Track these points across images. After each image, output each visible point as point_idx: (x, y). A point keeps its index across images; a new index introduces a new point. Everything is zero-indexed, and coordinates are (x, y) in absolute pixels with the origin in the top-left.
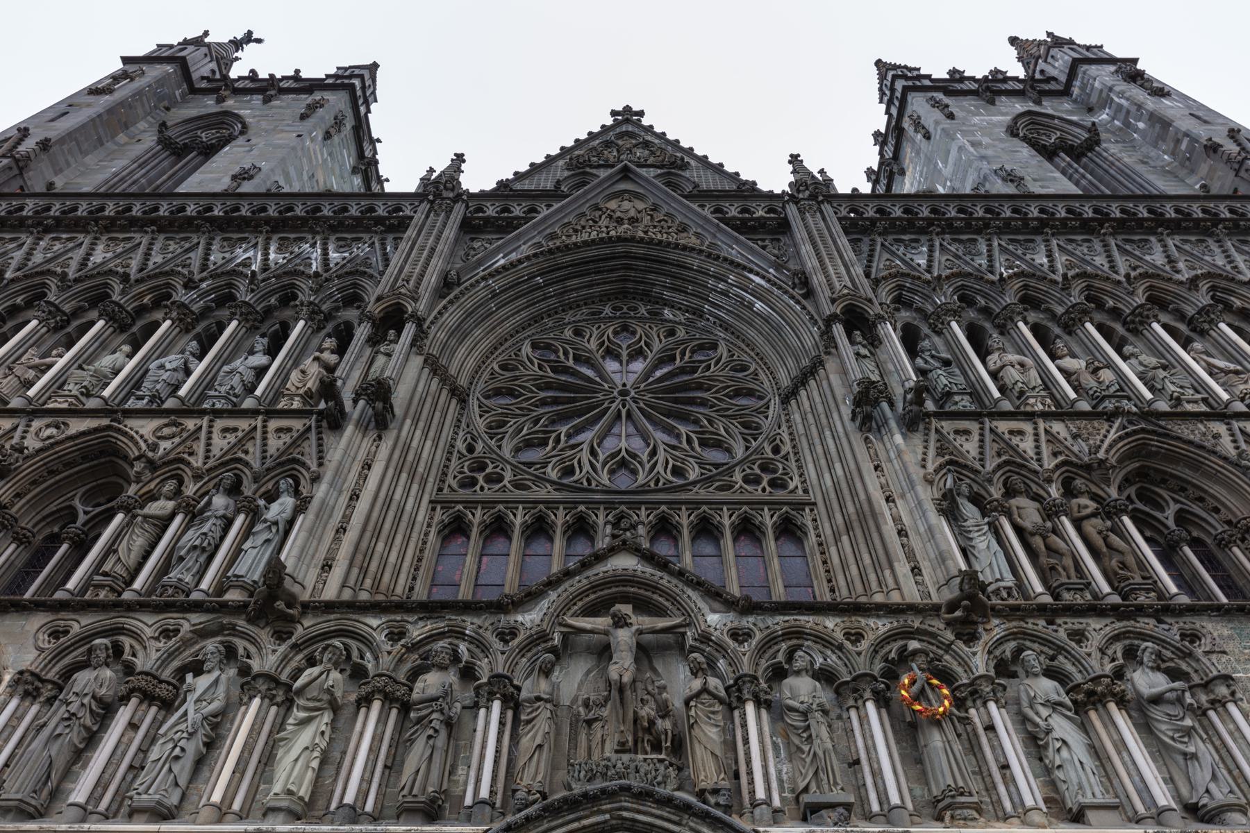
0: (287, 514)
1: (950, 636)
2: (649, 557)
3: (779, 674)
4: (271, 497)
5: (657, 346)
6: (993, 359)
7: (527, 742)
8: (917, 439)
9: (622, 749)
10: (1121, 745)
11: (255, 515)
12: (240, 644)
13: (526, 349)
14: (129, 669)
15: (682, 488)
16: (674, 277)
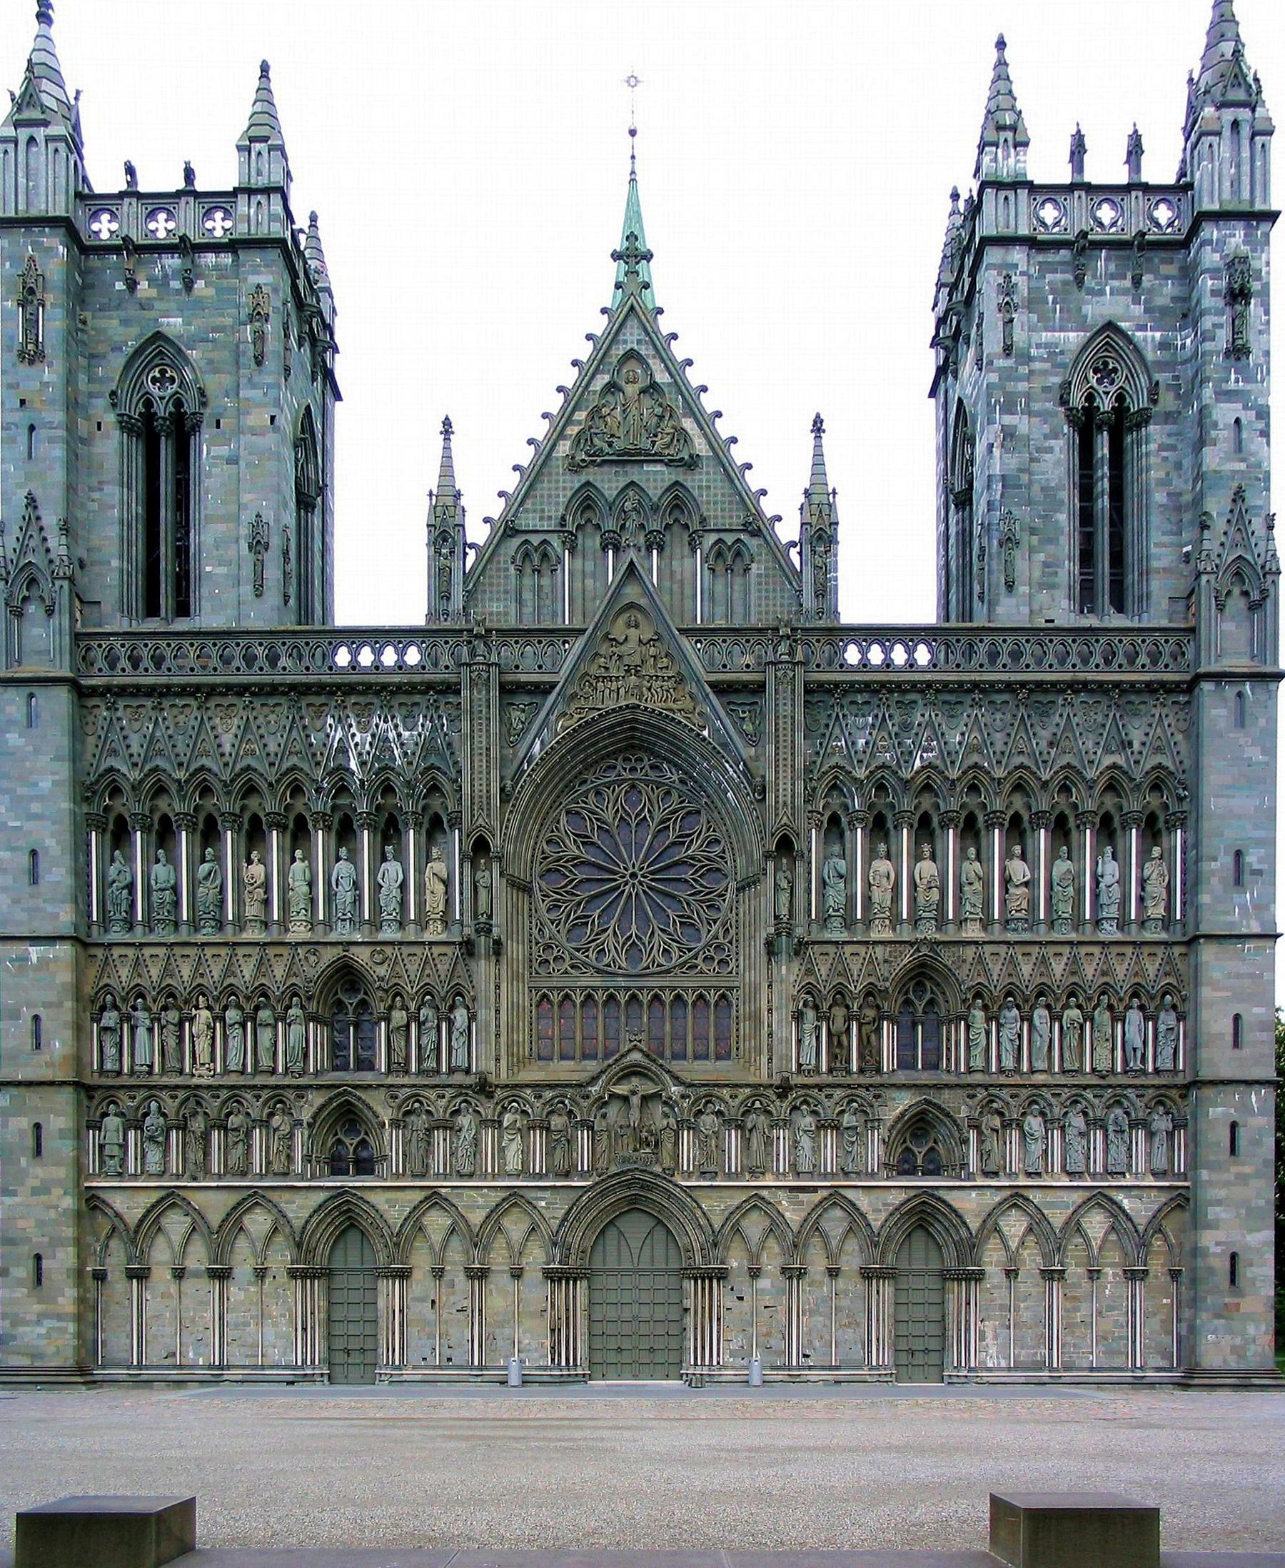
0: (466, 1024)
1: (774, 1098)
2: (647, 1056)
3: (700, 1112)
4: (452, 1008)
5: (658, 816)
6: (876, 864)
7: (599, 1150)
8: (795, 965)
9: (635, 1150)
10: (826, 1146)
11: (451, 1024)
12: (473, 1101)
13: (563, 819)
14: (428, 1112)
15: (668, 971)
16: (671, 743)
